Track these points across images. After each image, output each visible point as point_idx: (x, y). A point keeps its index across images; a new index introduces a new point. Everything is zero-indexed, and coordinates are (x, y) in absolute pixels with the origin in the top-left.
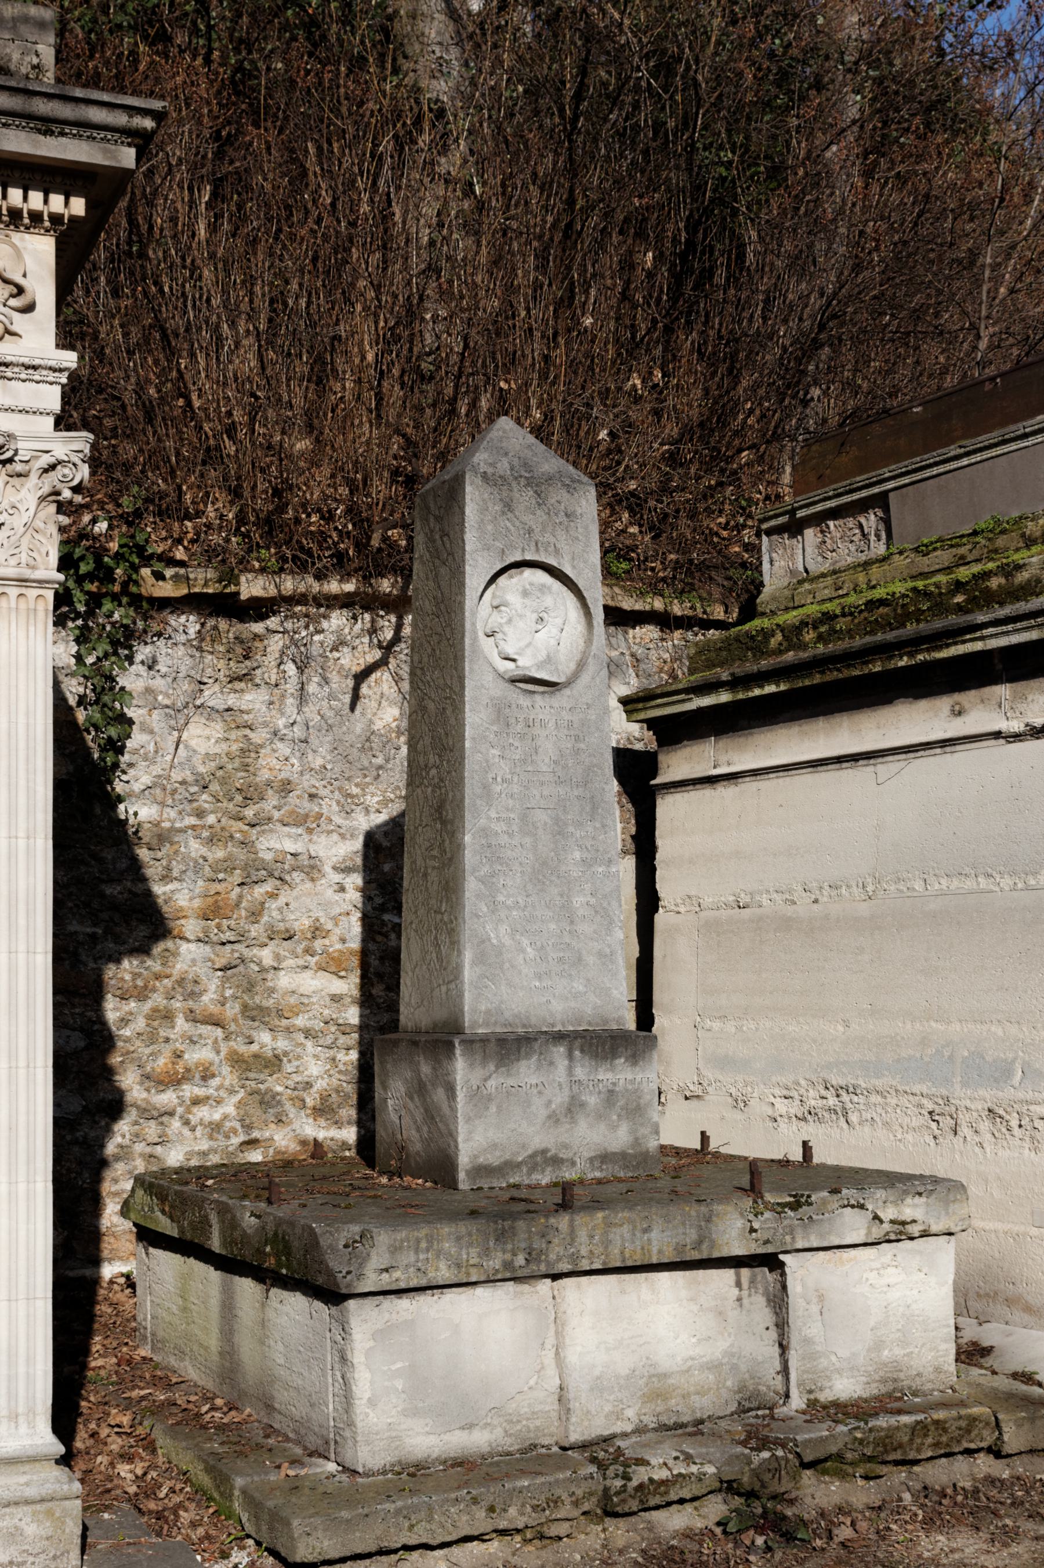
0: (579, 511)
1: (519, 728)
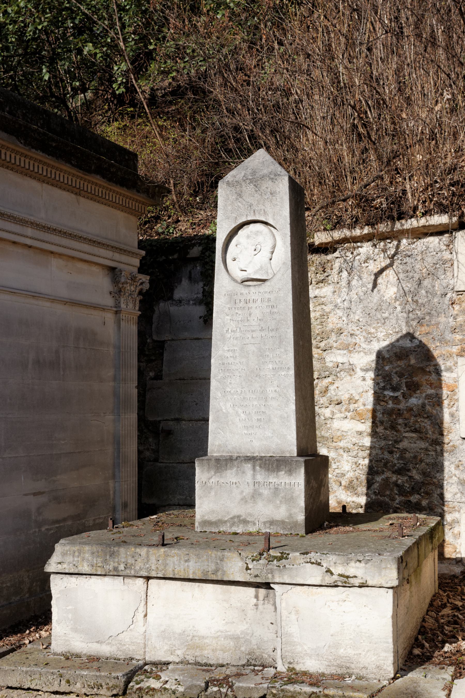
0: (278, 190)
1: (241, 305)
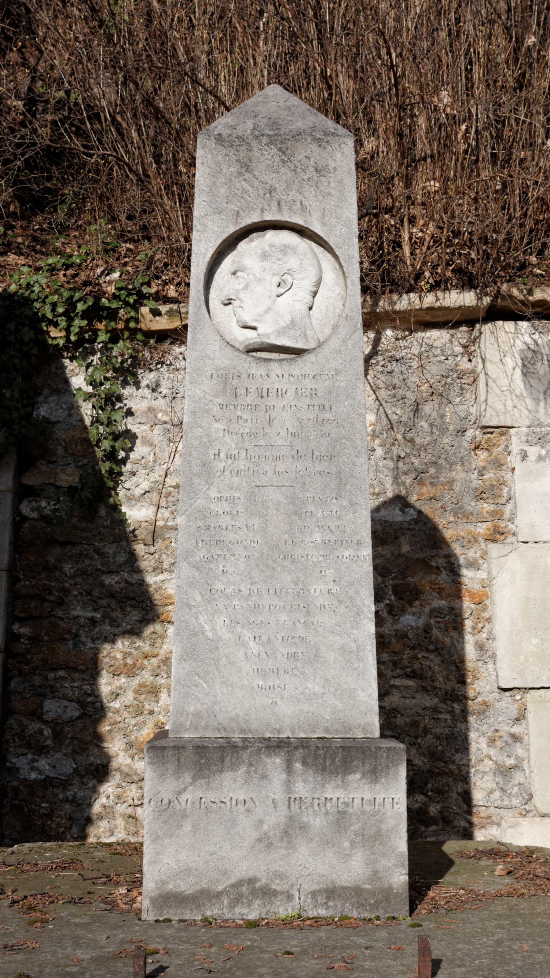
0: (332, 164)
1: (249, 399)
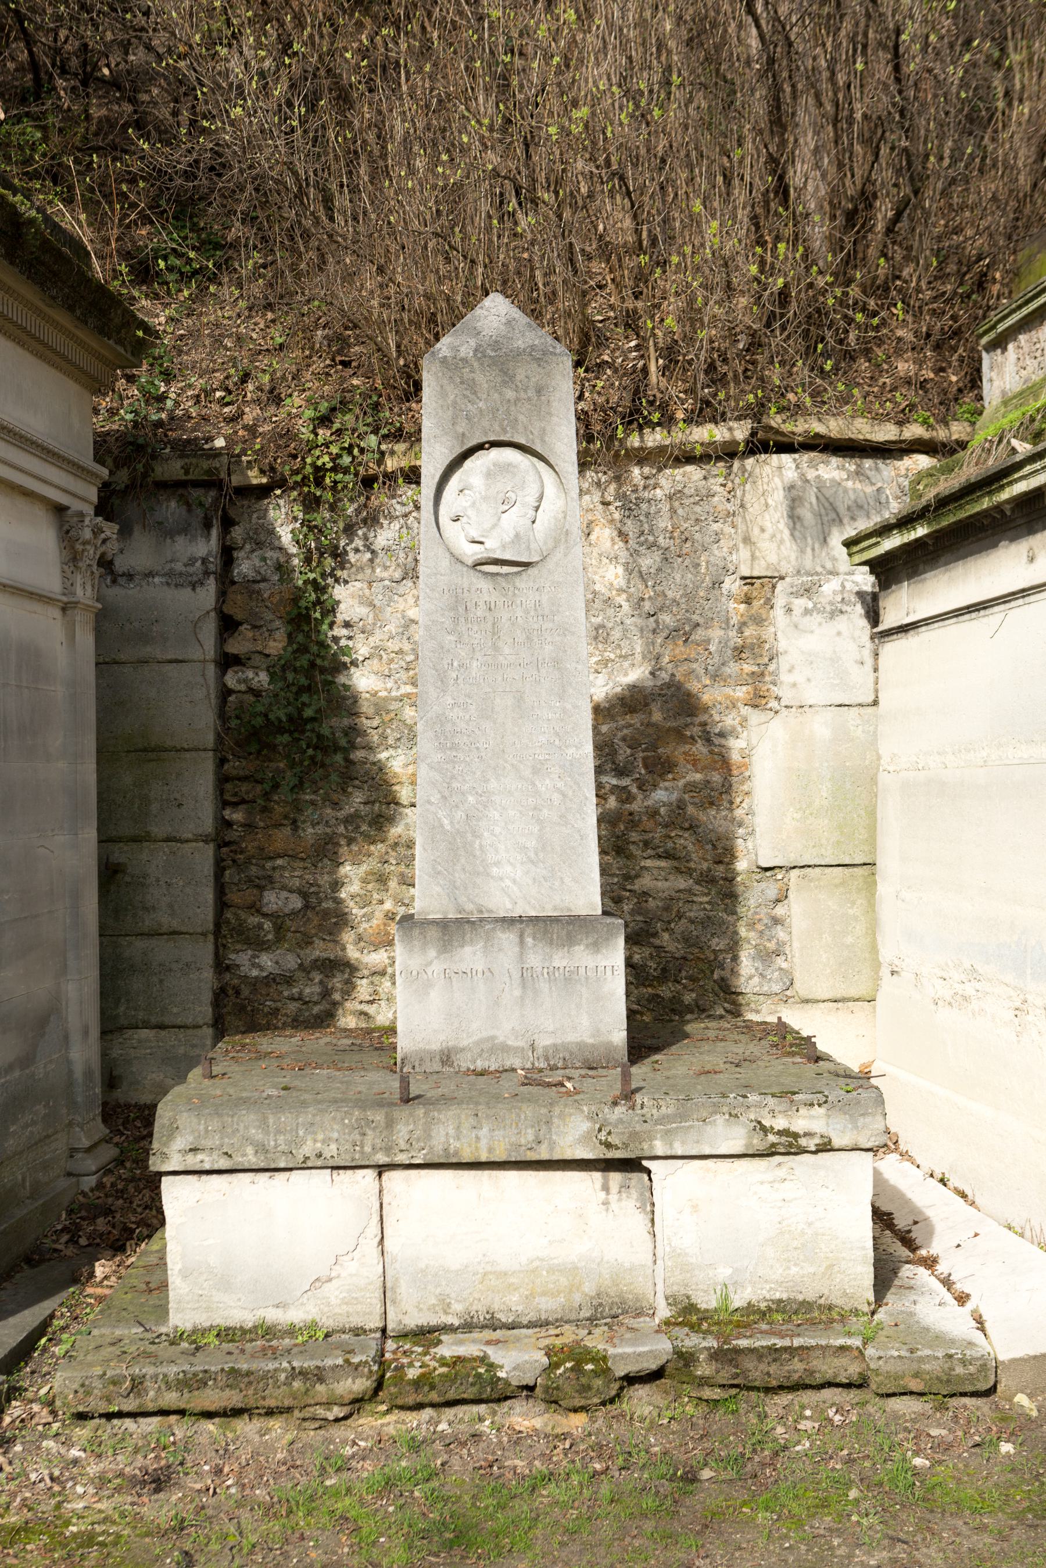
1: (479, 613)
